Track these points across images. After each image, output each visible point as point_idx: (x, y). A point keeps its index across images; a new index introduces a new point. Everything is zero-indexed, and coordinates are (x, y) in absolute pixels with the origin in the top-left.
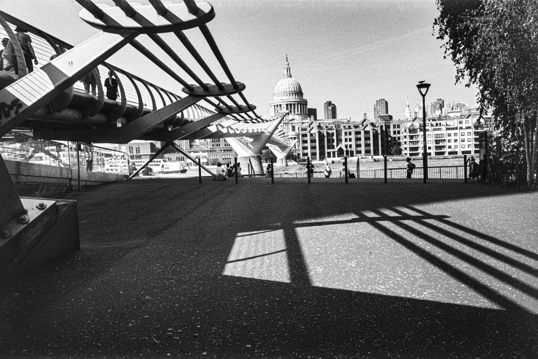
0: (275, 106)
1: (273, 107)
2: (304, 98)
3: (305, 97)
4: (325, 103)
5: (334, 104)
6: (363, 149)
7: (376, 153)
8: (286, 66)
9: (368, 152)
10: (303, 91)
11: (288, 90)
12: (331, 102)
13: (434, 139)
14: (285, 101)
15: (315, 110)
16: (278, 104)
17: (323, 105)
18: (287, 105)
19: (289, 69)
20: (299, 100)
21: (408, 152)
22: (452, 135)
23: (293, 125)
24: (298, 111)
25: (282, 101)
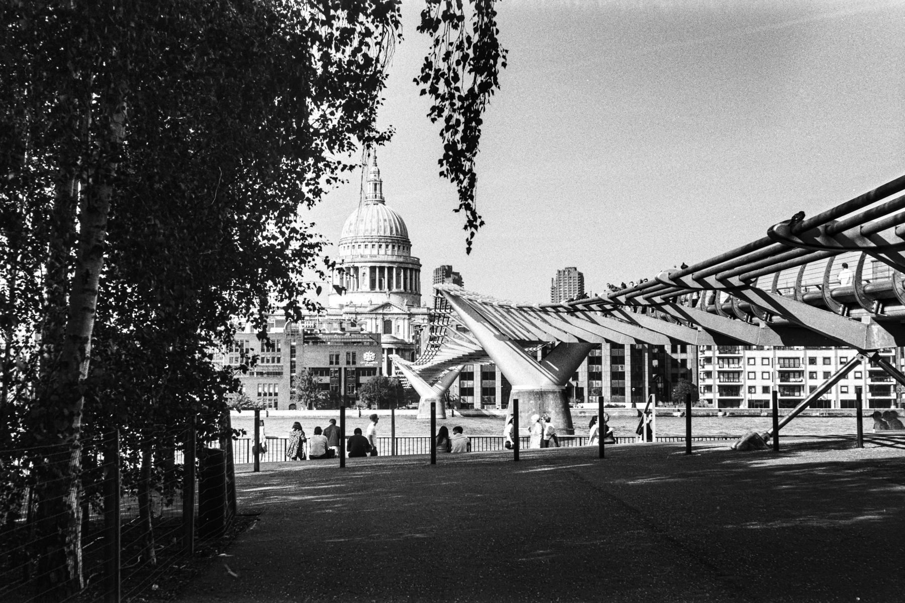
3: (414, 253)
4: (437, 271)
5: (457, 274)
6: (606, 383)
7: (637, 396)
8: (372, 177)
9: (618, 391)
11: (375, 233)
12: (450, 267)
13: (778, 368)
14: (369, 259)
17: (431, 275)
18: (373, 269)
19: (378, 185)
20: (401, 260)
21: (715, 396)
22: (820, 361)
23: (387, 318)
24: (398, 286)
25: (359, 259)
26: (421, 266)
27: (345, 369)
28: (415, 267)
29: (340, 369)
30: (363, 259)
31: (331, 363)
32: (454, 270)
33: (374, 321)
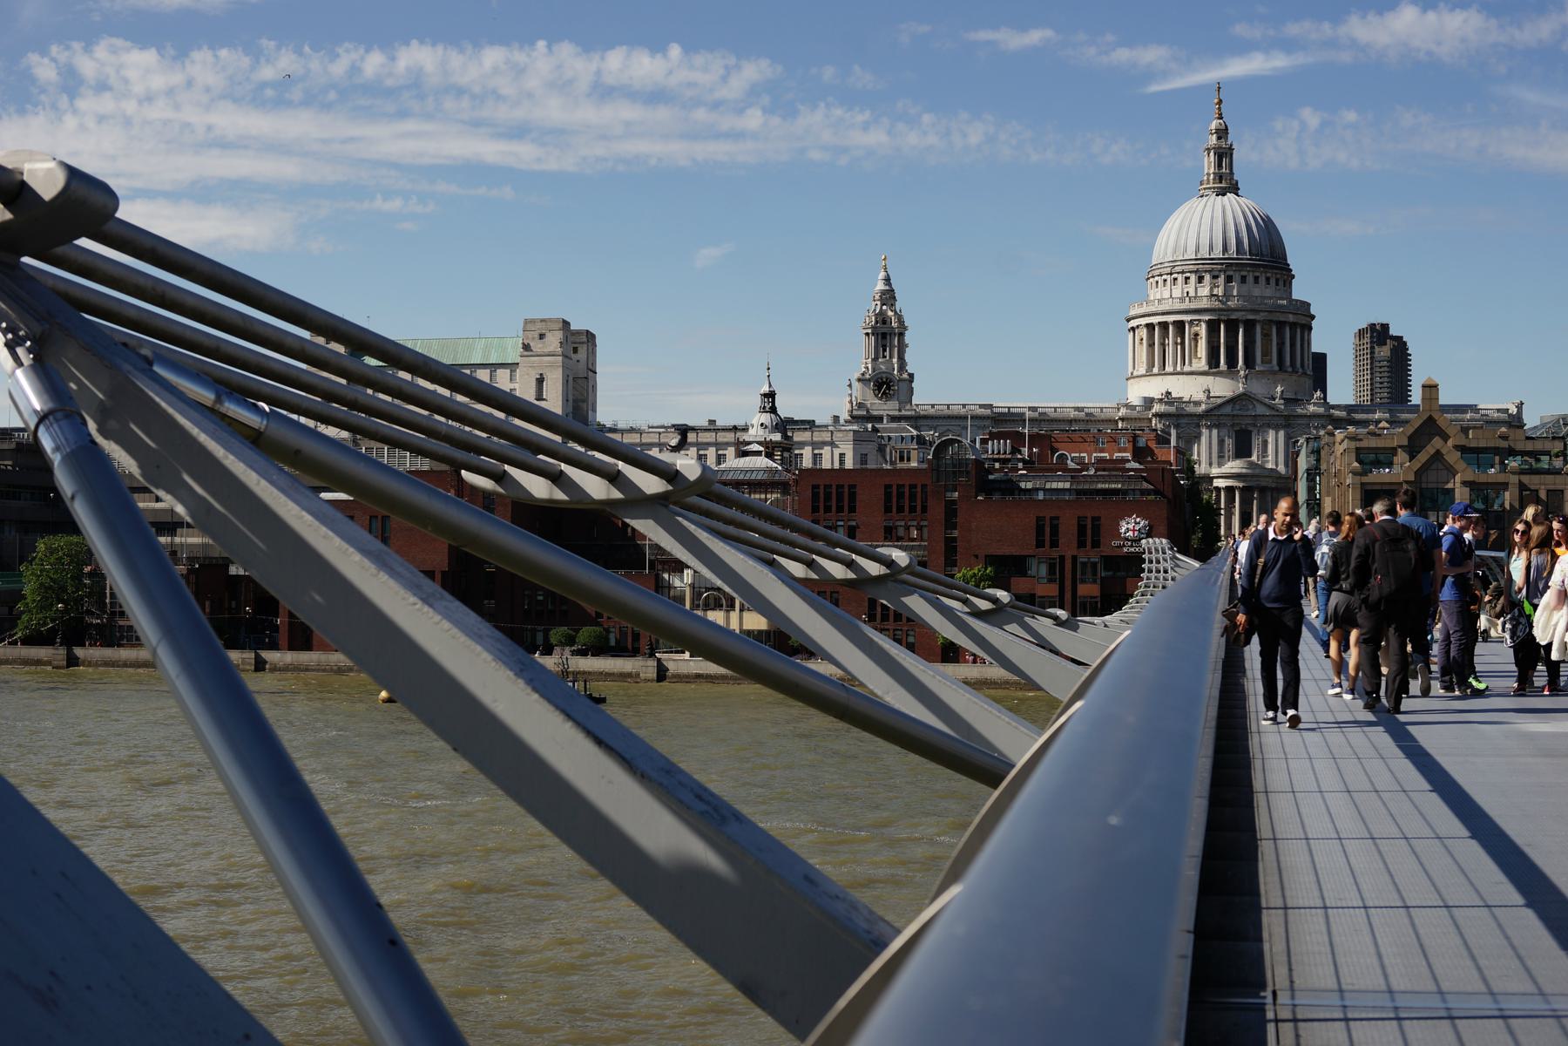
0: (1150, 327)
1: (1144, 333)
2: (1297, 294)
3: (1299, 292)
4: (1361, 333)
8: (1213, 139)
10: (1292, 260)
12: (1385, 327)
14: (1204, 304)
15: (1324, 356)
16: (1171, 318)
18: (1213, 327)
19: (1224, 155)
25: (1186, 305)
26: (1313, 317)
27: (1074, 558)
28: (1303, 320)
29: (1062, 558)
30: (1193, 306)
31: (1040, 544)
32: (1393, 332)
33: (1215, 432)
